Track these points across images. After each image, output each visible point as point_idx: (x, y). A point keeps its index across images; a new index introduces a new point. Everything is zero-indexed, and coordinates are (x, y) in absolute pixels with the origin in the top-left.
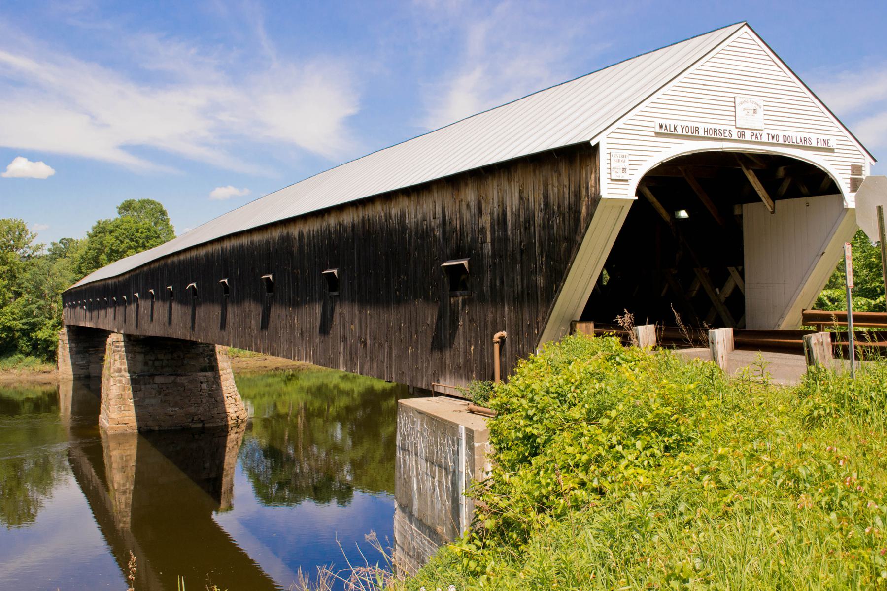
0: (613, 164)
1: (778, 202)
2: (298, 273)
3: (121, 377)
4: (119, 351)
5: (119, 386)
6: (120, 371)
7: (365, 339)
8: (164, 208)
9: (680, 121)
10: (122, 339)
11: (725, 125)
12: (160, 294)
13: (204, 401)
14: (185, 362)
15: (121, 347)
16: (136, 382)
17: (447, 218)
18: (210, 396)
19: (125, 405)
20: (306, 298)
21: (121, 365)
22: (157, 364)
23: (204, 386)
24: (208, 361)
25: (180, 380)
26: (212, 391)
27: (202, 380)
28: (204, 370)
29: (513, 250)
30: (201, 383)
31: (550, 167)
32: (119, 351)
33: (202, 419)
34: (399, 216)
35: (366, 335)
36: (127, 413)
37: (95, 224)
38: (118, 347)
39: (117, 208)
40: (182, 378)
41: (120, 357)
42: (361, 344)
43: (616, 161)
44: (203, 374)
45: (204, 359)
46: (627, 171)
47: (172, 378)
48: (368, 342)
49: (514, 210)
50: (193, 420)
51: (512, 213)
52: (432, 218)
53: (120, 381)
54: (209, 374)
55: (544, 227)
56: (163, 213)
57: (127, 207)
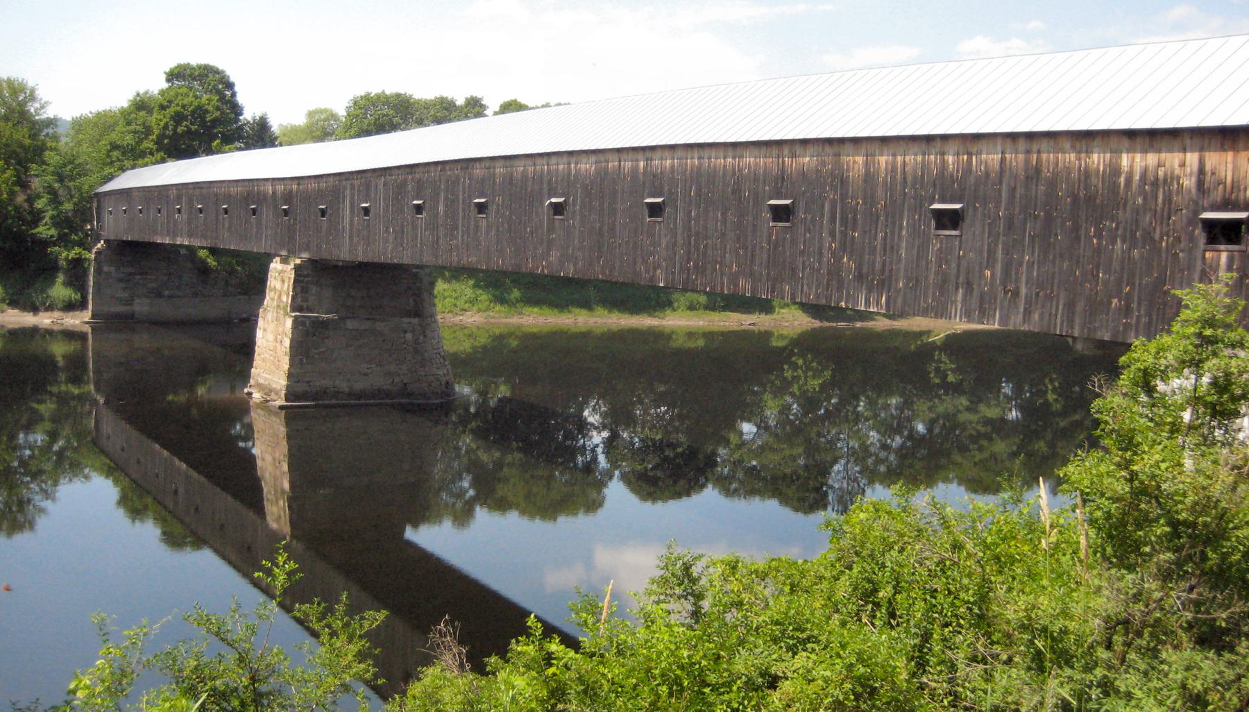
2: (858, 203)
8: (232, 79)
12: (441, 208)
18: (416, 351)
23: (409, 336)
25: (380, 326)
26: (418, 344)
28: (408, 314)
30: (405, 332)
33: (405, 381)
39: (165, 73)
40: (383, 324)
42: (1006, 293)
44: (406, 320)
48: (1023, 291)
50: (393, 382)
52: (1176, 166)
54: (415, 321)
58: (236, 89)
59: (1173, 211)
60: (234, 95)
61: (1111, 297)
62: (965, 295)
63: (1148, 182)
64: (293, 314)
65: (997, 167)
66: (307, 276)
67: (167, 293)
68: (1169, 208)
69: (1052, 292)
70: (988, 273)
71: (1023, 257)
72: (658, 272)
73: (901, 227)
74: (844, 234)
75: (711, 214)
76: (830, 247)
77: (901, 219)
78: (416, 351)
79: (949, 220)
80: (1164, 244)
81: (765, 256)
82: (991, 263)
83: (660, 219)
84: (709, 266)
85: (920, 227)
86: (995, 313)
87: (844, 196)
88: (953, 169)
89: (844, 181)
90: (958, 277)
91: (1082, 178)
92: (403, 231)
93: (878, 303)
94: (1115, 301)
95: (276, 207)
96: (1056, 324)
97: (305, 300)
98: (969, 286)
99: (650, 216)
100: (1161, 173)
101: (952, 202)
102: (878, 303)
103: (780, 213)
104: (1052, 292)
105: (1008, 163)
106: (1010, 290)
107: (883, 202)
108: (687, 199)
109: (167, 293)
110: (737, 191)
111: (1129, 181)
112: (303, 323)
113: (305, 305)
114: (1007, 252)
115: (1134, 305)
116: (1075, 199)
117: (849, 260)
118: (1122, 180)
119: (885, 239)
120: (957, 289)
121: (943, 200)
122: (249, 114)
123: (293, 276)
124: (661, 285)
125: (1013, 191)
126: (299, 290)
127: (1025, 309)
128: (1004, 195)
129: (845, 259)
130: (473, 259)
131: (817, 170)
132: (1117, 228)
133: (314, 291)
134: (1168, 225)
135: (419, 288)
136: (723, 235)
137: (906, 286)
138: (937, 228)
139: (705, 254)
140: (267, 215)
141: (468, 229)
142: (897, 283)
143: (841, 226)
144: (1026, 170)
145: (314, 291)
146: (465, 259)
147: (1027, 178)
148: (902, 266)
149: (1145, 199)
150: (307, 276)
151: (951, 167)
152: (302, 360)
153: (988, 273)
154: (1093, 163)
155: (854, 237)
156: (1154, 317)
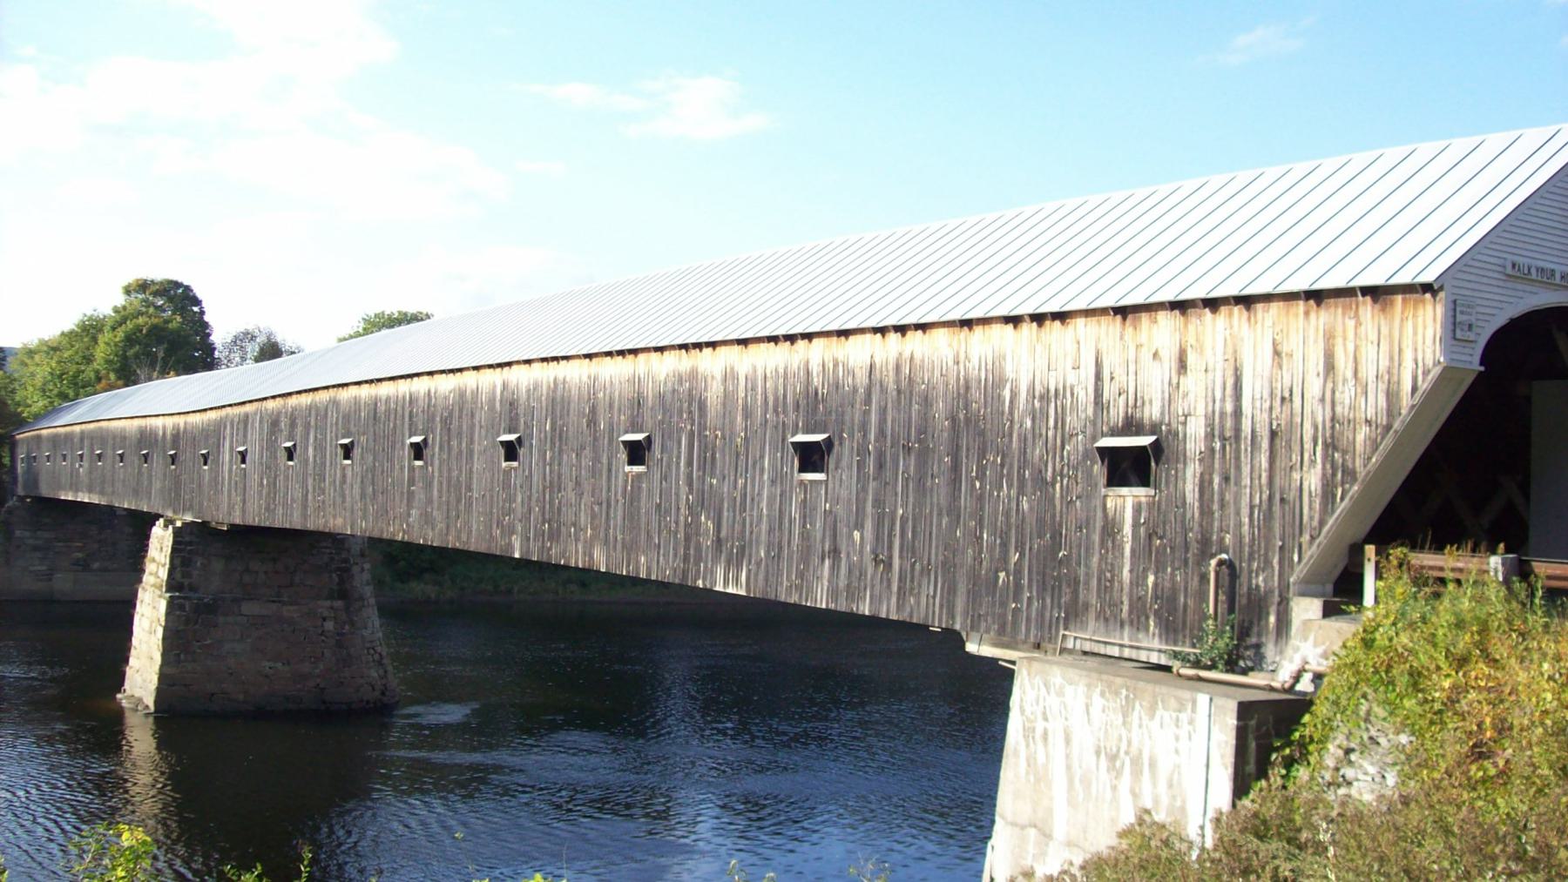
0: (1460, 318)
2: (716, 436)
3: (184, 598)
5: (179, 616)
7: (890, 557)
13: (327, 653)
14: (297, 579)
20: (736, 481)
21: (183, 577)
22: (247, 579)
23: (329, 625)
24: (337, 580)
25: (289, 611)
27: (326, 614)
29: (1253, 431)
30: (324, 619)
31: (1340, 311)
34: (990, 363)
35: (890, 548)
40: (291, 608)
43: (1462, 313)
45: (331, 577)
46: (1474, 328)
47: (274, 606)
54: (339, 604)
55: (1322, 400)
58: (204, 304)
59: (1067, 436)
60: (202, 313)
61: (997, 572)
62: (832, 568)
63: (1037, 394)
64: (168, 595)
65: (866, 381)
66: (190, 543)
67: (96, 565)
68: (1063, 436)
69: (929, 564)
70: (857, 535)
71: (894, 512)
72: (514, 537)
73: (762, 470)
74: (702, 479)
75: (565, 457)
76: (688, 499)
77: (762, 457)
78: (339, 644)
79: (811, 457)
80: (1058, 486)
81: (620, 513)
82: (859, 526)
83: (515, 464)
84: (563, 529)
85: (782, 468)
86: (865, 595)
87: (703, 427)
88: (818, 381)
89: (702, 406)
90: (823, 541)
91: (962, 391)
92: (275, 484)
93: (737, 581)
94: (1002, 575)
95: (165, 452)
96: (934, 612)
97: (186, 575)
98: (835, 552)
99: (506, 460)
101: (813, 432)
102: (737, 581)
103: (636, 453)
104: (929, 564)
105: (878, 372)
106: (882, 561)
107: (743, 434)
108: (542, 435)
109: (96, 565)
110: (592, 422)
111: (1014, 395)
112: (182, 607)
113: (186, 582)
114: (878, 503)
115: (1025, 582)
116: (953, 419)
117: (707, 518)
118: (1007, 394)
120: (823, 560)
121: (807, 431)
122: (220, 336)
123: (170, 544)
124: (517, 555)
125: (883, 412)
126: (178, 562)
127: (899, 588)
128: (874, 418)
129: (703, 518)
130: (339, 521)
131: (674, 391)
132: (1002, 465)
133: (199, 564)
134: (1062, 458)
135: (346, 561)
136: (578, 483)
137: (768, 552)
138: (802, 469)
139: (559, 509)
140: (157, 461)
141: (335, 481)
142: (758, 552)
143: (699, 470)
144: (898, 382)
145: (199, 564)
146: (331, 521)
147: (899, 392)
148: (764, 527)
149: (1033, 420)
150: (190, 543)
151: (815, 380)
154: (974, 369)
155: (711, 485)
156: (1048, 601)
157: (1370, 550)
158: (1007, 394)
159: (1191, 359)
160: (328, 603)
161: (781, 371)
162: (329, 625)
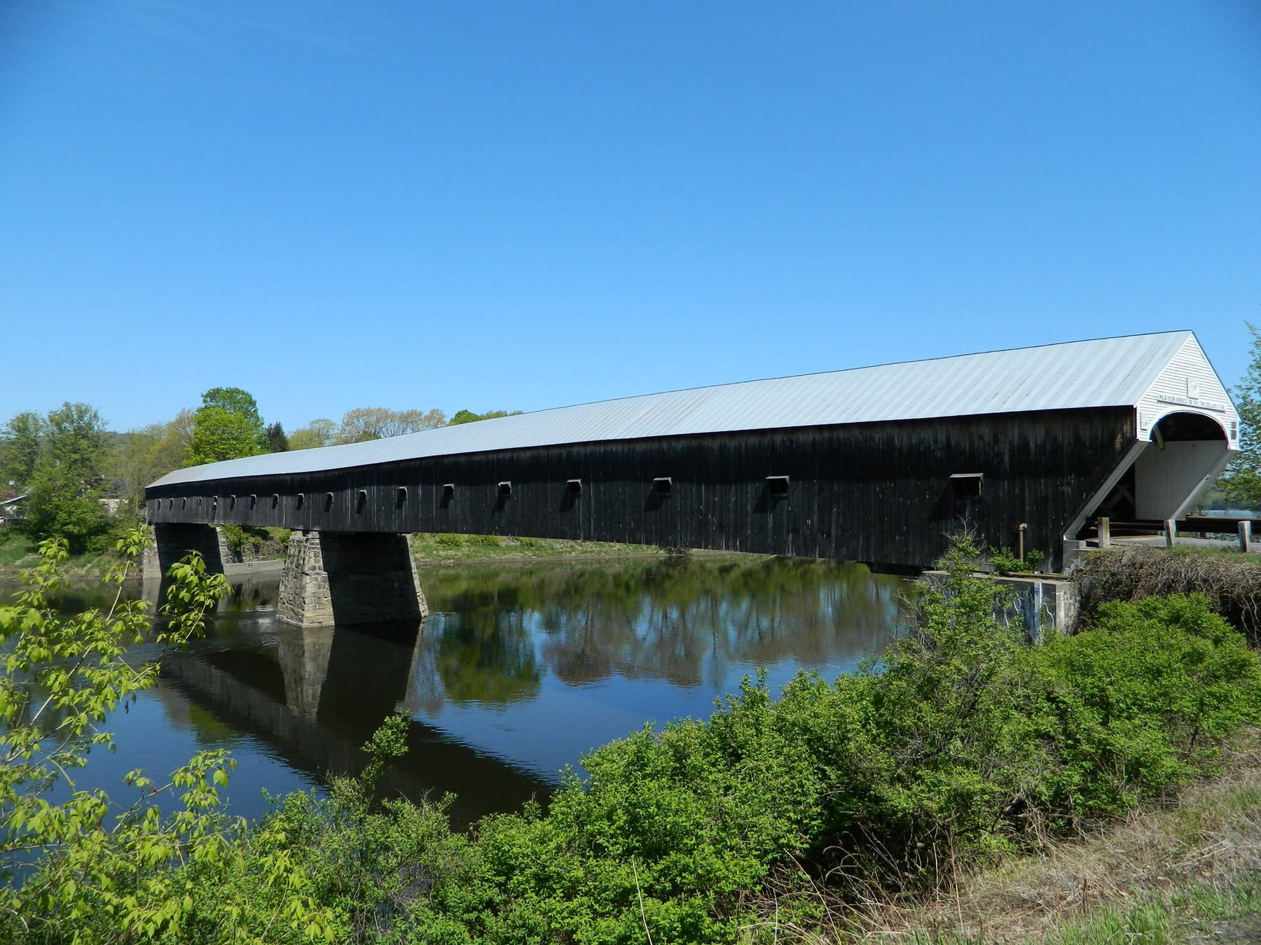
1: (1168, 443)
4: (314, 548)
6: (314, 568)
8: (254, 398)
9: (1168, 396)
10: (318, 536)
11: (1179, 396)
15: (317, 544)
16: (334, 579)
17: (953, 444)
19: (320, 604)
23: (396, 585)
30: (393, 582)
32: (314, 548)
36: (321, 612)
37: (178, 411)
38: (313, 544)
41: (315, 554)
49: (1039, 442)
51: (1036, 445)
53: (316, 579)
54: (400, 573)
56: (253, 403)
57: (214, 395)
100: (921, 449)
118: (896, 454)
119: (736, 501)
120: (788, 534)
127: (836, 544)
137: (752, 532)
152: (315, 606)
153: (809, 522)
157: (1106, 520)
158: (896, 454)
159: (1001, 437)
160: (394, 573)
161: (757, 446)
162: (396, 585)
